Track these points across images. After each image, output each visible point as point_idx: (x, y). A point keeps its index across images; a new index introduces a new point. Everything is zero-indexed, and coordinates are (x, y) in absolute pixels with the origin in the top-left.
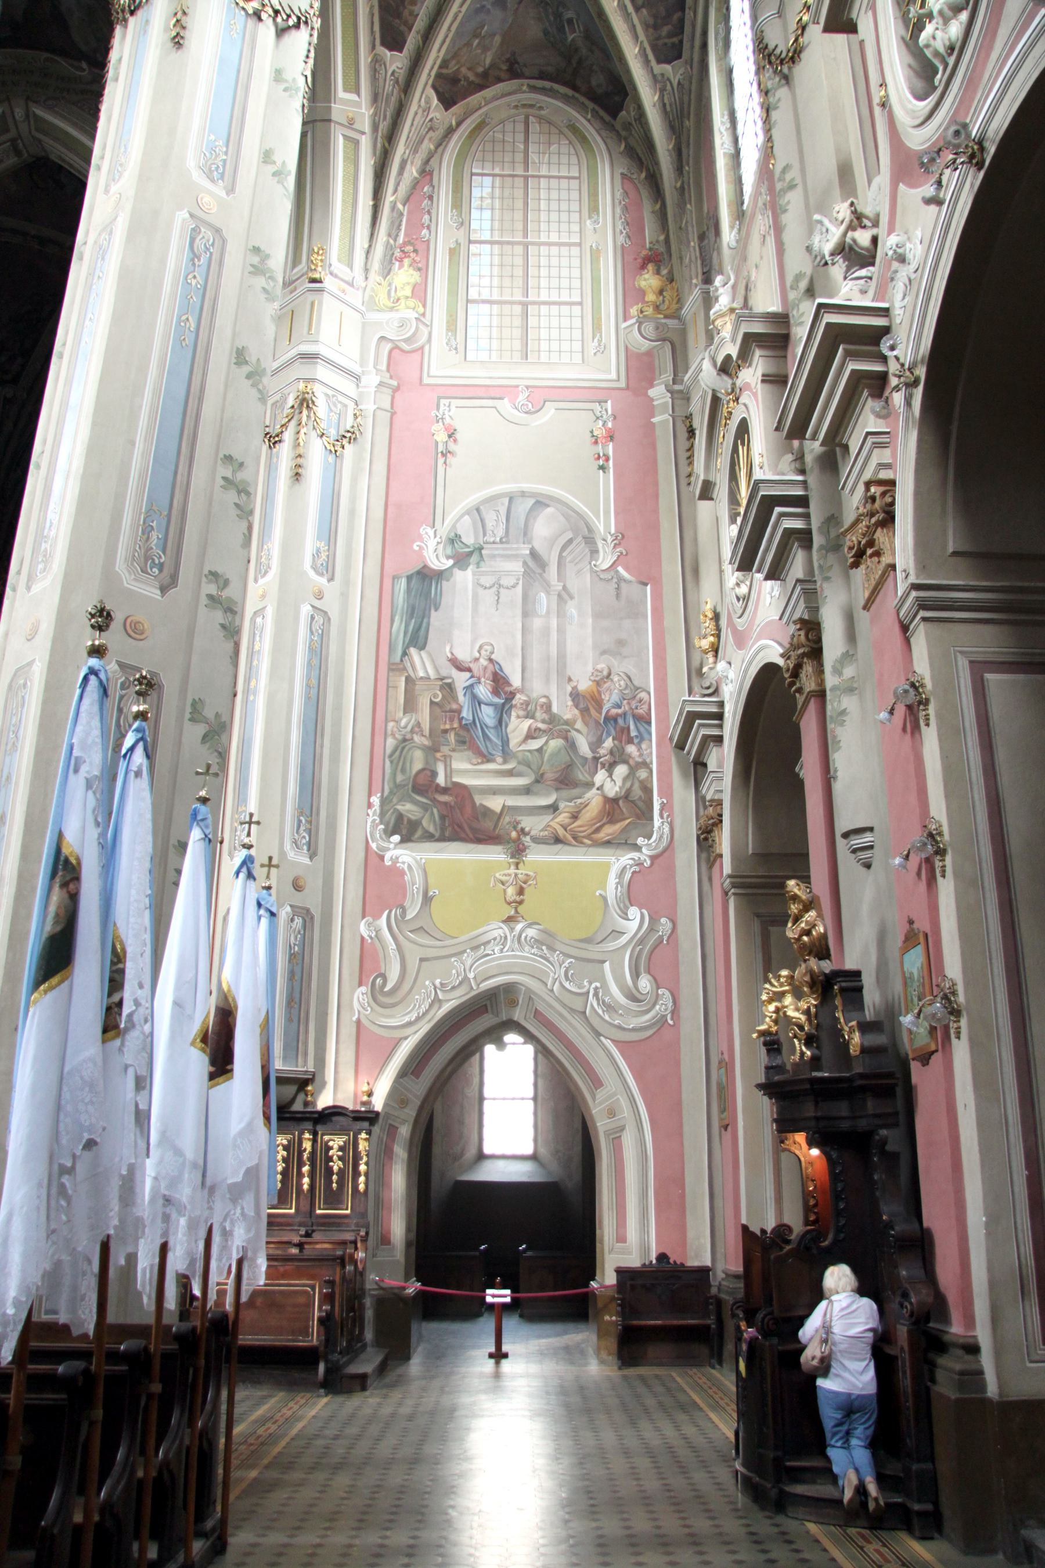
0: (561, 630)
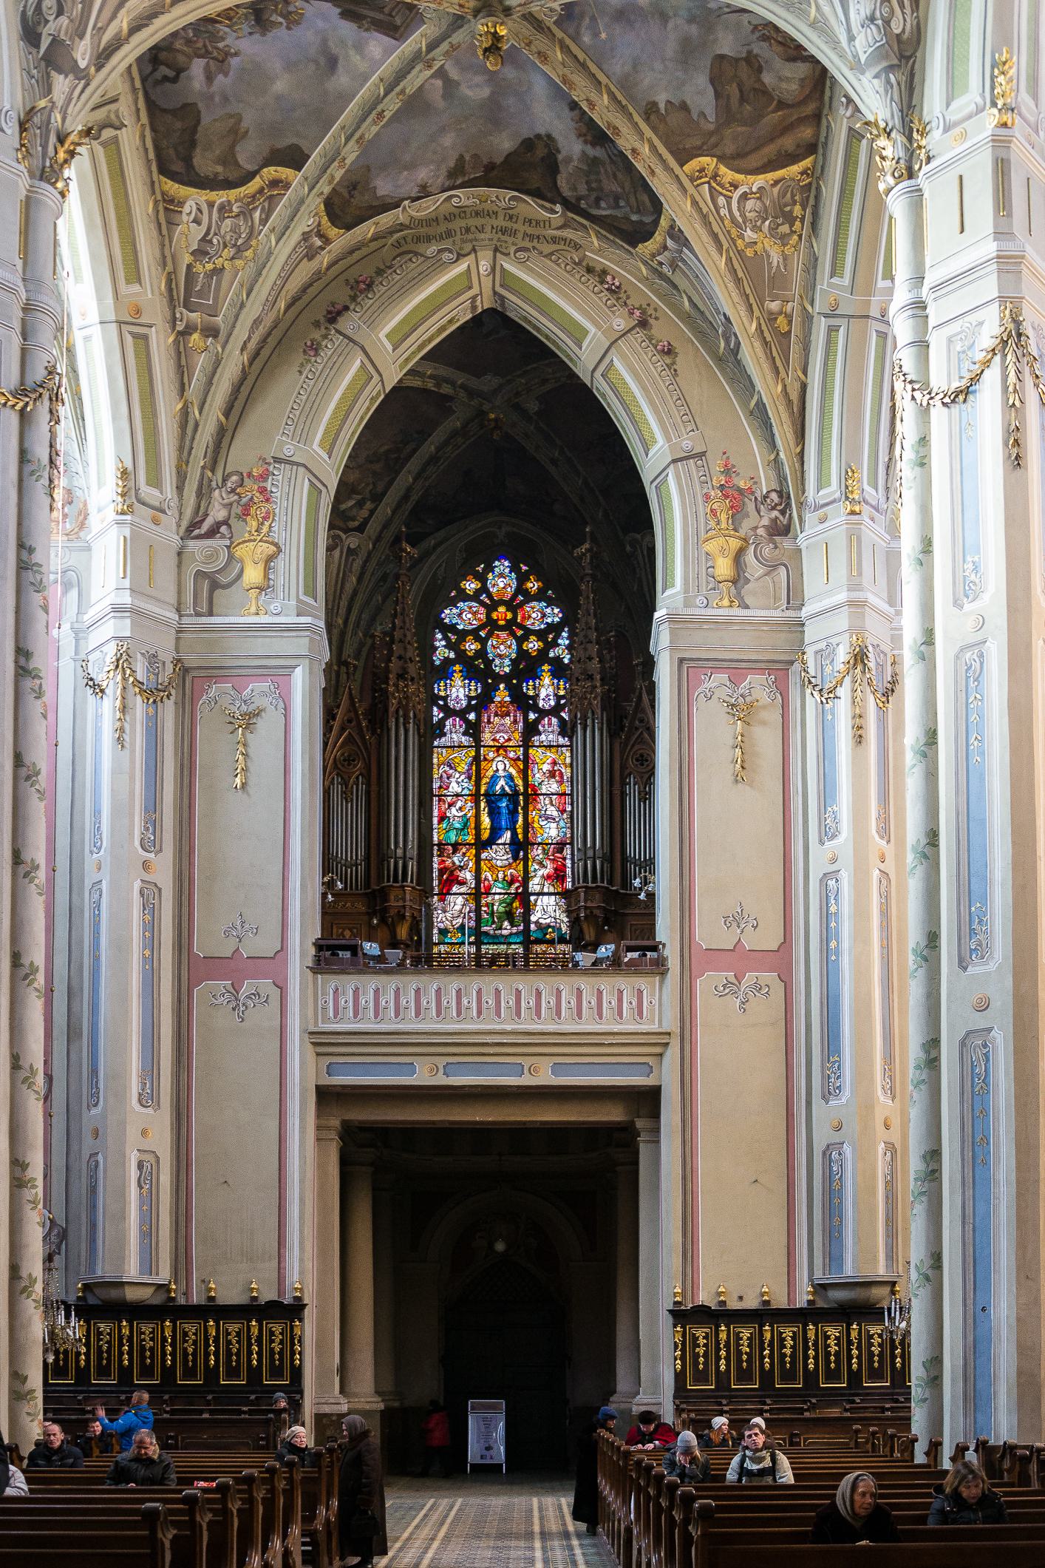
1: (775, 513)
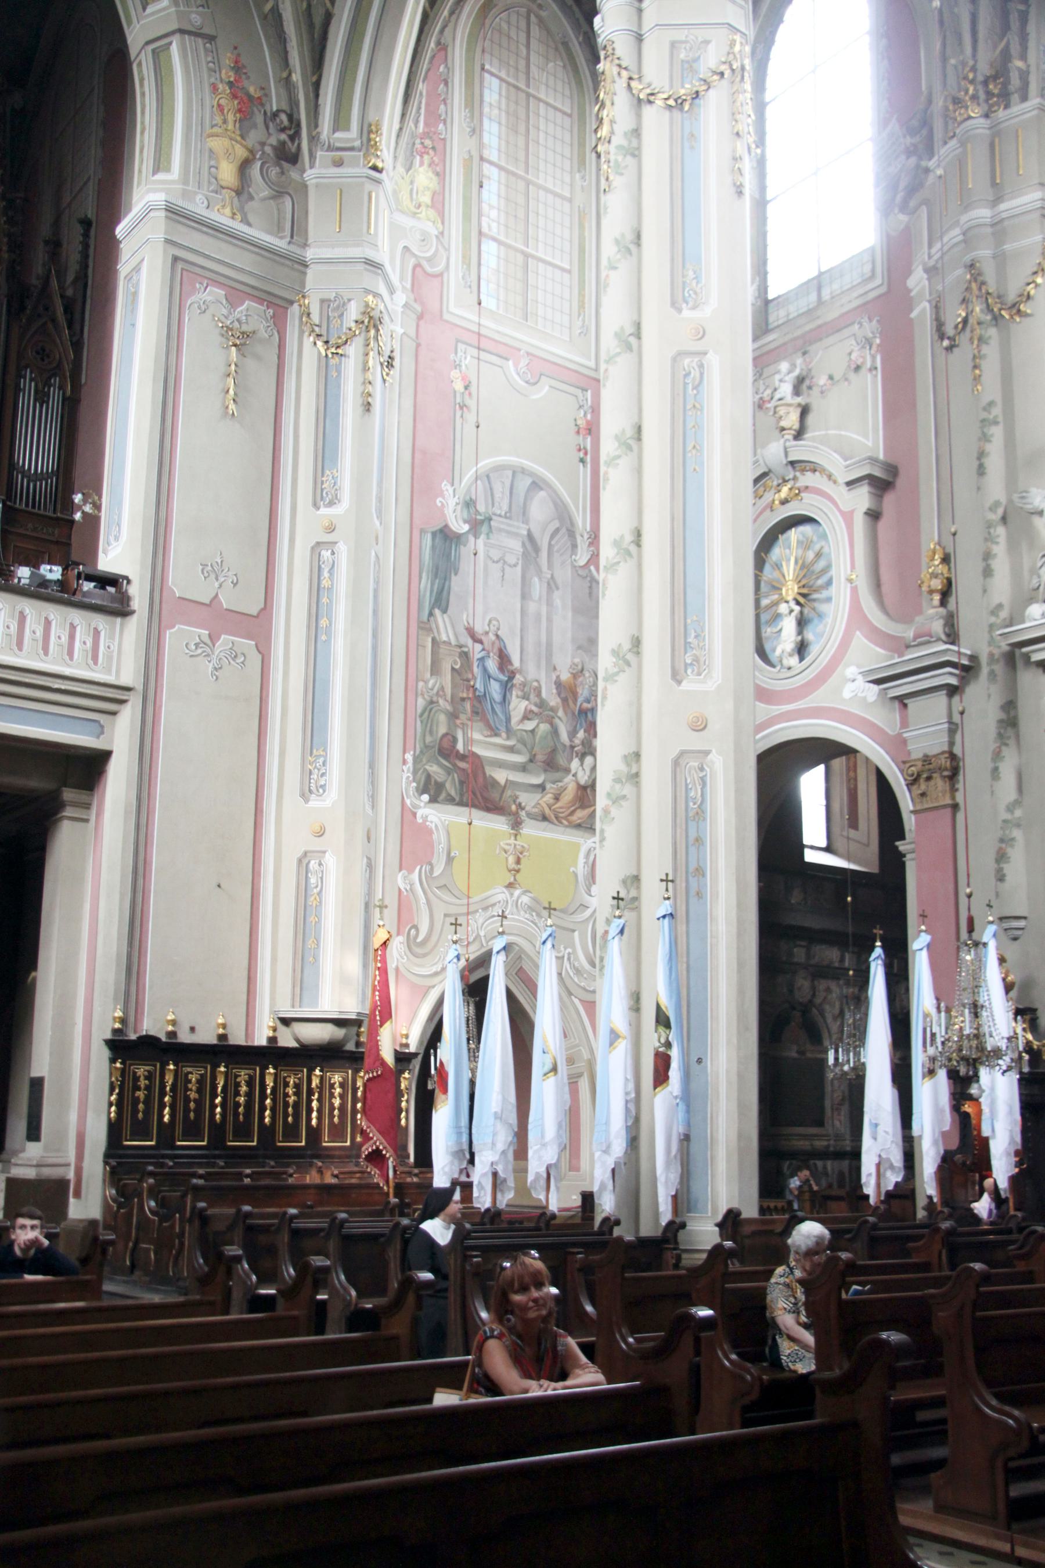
0: (549, 620)
1: (283, 137)
